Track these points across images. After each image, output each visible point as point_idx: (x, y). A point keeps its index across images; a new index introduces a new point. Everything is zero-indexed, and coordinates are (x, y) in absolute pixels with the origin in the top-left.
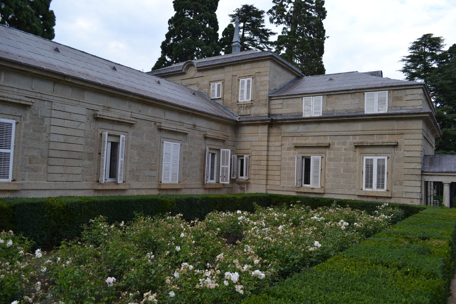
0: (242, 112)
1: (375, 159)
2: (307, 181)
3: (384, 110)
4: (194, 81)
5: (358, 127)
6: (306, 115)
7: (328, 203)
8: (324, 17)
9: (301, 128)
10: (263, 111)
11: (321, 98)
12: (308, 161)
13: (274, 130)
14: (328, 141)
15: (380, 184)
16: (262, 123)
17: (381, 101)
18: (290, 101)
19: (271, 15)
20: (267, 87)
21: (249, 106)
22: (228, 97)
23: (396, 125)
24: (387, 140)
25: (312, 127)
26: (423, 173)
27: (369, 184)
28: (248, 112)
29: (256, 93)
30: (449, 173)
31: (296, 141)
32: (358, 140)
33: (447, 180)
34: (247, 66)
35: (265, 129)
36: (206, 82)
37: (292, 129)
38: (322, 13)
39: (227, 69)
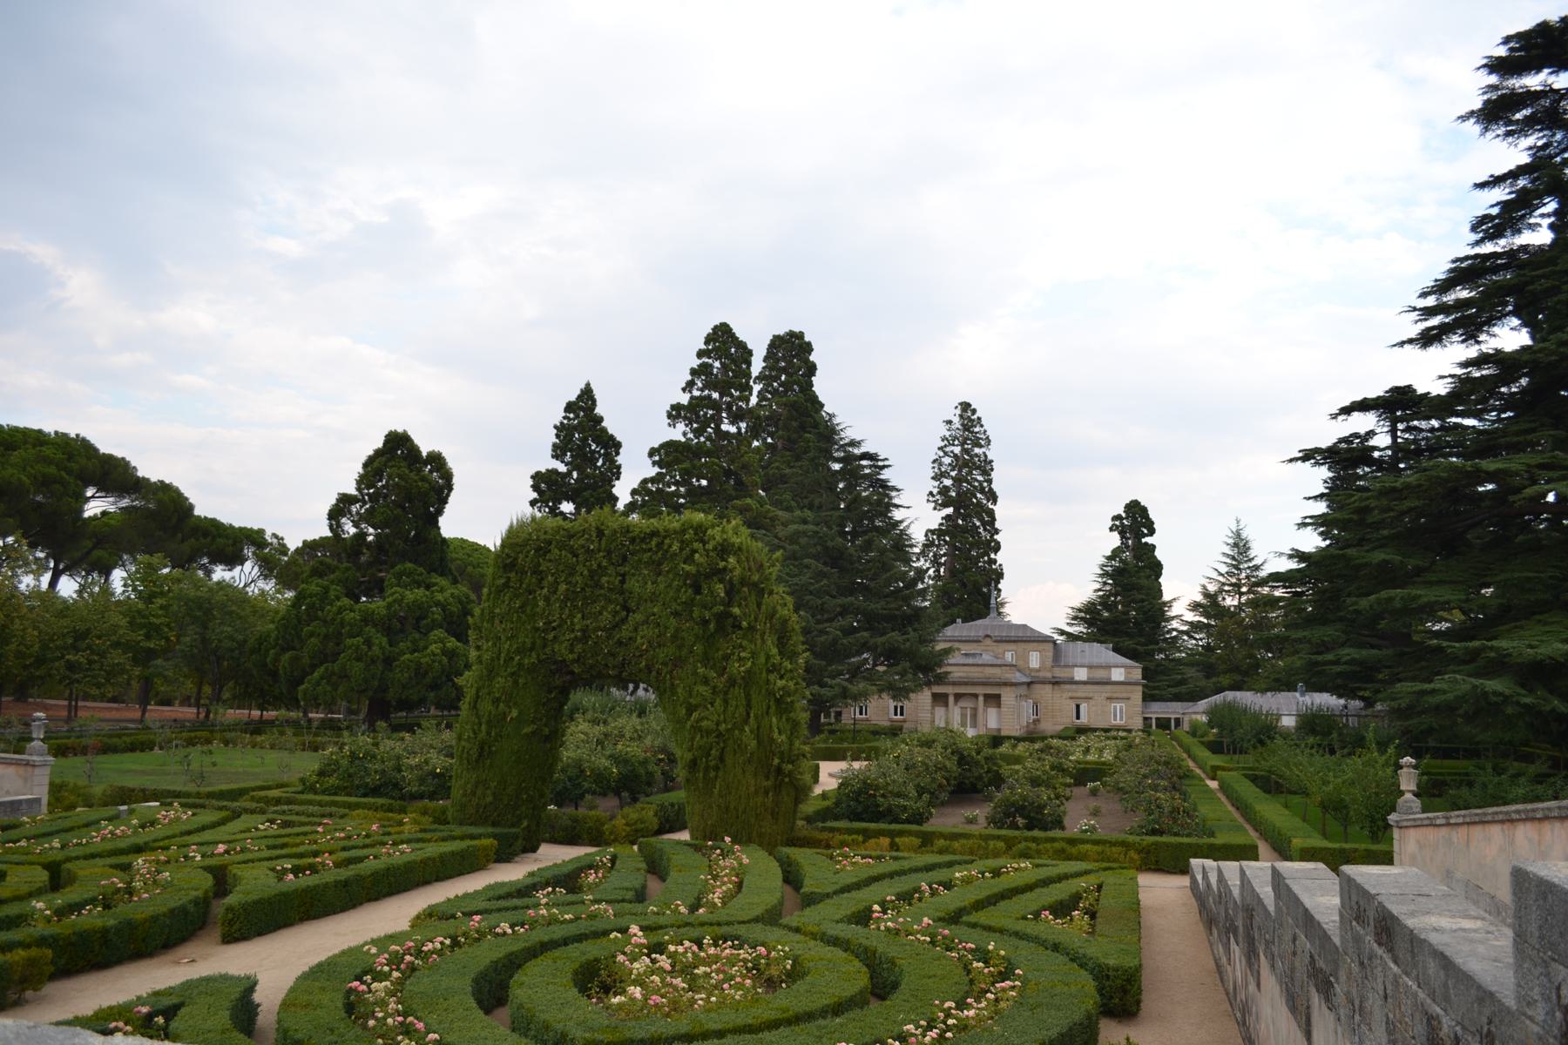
0: (1033, 674)
1: (1118, 705)
2: (1078, 718)
3: (1122, 679)
4: (989, 648)
5: (1108, 687)
6: (1077, 678)
7: (1095, 730)
8: (995, 502)
9: (1074, 687)
10: (1049, 675)
11: (1085, 669)
12: (1078, 707)
13: (1056, 687)
14: (1091, 695)
15: (1121, 719)
16: (1050, 683)
17: (1121, 674)
18: (1066, 670)
19: (931, 499)
20: (1051, 660)
21: (1038, 671)
22: (1020, 663)
23: (1129, 687)
24: (1125, 695)
25: (1081, 686)
26: (1143, 713)
27: (1115, 720)
28: (1037, 674)
29: (1042, 662)
30: (1155, 713)
31: (1070, 694)
32: (1108, 695)
33: (1154, 716)
34: (1035, 644)
35: (1051, 686)
36: (1000, 651)
37: (1068, 686)
38: (993, 497)
39: (1019, 644)
